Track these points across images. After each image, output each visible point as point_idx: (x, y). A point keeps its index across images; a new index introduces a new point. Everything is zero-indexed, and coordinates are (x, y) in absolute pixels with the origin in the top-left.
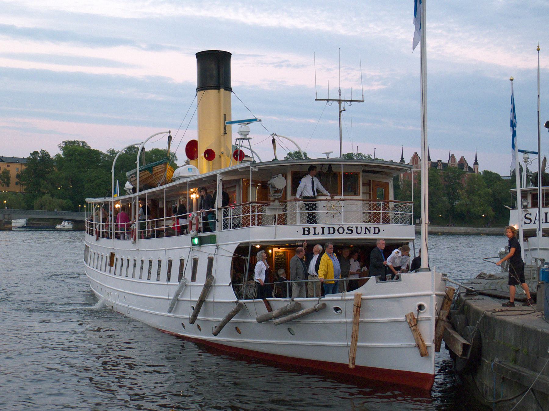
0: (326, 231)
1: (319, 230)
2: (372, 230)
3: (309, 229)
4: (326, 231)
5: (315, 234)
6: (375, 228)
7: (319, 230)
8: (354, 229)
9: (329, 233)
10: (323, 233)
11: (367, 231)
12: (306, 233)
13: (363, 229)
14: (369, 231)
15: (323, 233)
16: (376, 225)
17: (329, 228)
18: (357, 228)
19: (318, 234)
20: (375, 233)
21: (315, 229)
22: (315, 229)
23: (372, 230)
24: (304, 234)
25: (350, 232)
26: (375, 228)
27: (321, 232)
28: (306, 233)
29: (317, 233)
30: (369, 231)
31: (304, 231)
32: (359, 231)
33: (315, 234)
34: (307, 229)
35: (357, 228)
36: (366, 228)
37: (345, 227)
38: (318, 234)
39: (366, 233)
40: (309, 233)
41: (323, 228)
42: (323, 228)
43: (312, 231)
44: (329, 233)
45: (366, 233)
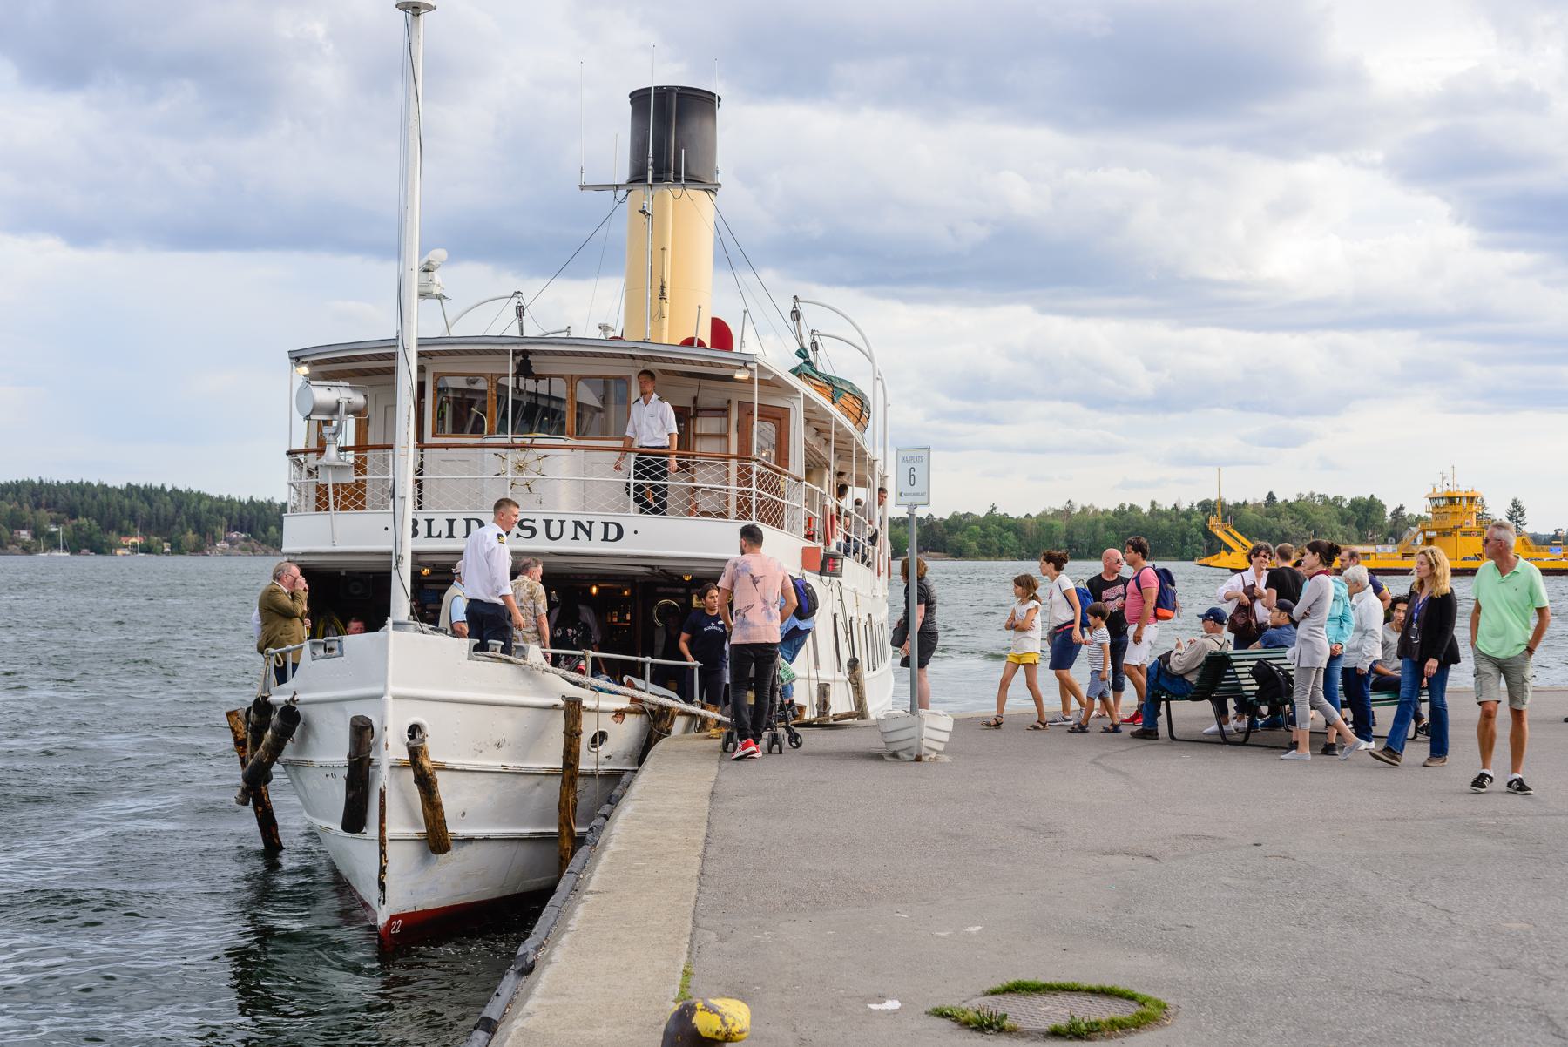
1: (440, 525)
2: (598, 531)
5: (430, 535)
6: (606, 525)
7: (440, 525)
8: (540, 527)
10: (451, 535)
13: (569, 528)
15: (451, 535)
18: (548, 522)
20: (605, 538)
21: (429, 522)
22: (429, 522)
23: (598, 531)
25: (528, 533)
26: (606, 525)
27: (445, 533)
29: (434, 533)
32: (555, 532)
33: (430, 535)
35: (548, 522)
36: (578, 523)
39: (575, 538)
41: (451, 522)
42: (451, 522)
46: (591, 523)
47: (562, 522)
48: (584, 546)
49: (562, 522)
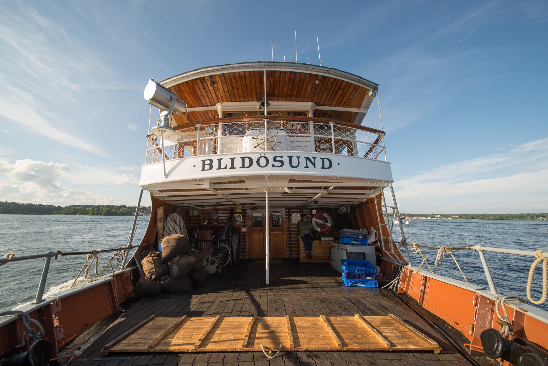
0: (238, 163)
2: (319, 163)
3: (211, 161)
4: (238, 163)
5: (220, 168)
6: (323, 159)
7: (226, 161)
8: (286, 160)
9: (243, 166)
10: (232, 167)
11: (309, 164)
12: (207, 167)
13: (303, 161)
14: (314, 164)
15: (232, 167)
16: (324, 155)
17: (243, 159)
18: (290, 158)
19: (226, 168)
20: (323, 167)
21: (220, 160)
22: (220, 160)
23: (319, 163)
24: (203, 169)
25: (279, 164)
26: (323, 159)
27: (229, 166)
28: (207, 167)
30: (314, 164)
31: (204, 164)
32: (295, 163)
34: (208, 162)
35: (290, 158)
36: (307, 159)
37: (270, 157)
38: (226, 168)
39: (307, 167)
40: (211, 167)
41: (233, 160)
42: (233, 160)
43: (216, 164)
44: (243, 166)
45: (307, 167)
46: (315, 158)
47: (298, 158)
48: (311, 172)
49: (298, 158)
